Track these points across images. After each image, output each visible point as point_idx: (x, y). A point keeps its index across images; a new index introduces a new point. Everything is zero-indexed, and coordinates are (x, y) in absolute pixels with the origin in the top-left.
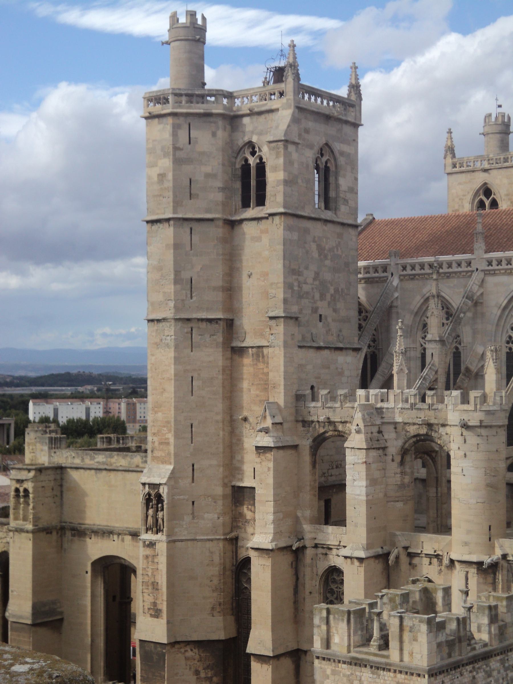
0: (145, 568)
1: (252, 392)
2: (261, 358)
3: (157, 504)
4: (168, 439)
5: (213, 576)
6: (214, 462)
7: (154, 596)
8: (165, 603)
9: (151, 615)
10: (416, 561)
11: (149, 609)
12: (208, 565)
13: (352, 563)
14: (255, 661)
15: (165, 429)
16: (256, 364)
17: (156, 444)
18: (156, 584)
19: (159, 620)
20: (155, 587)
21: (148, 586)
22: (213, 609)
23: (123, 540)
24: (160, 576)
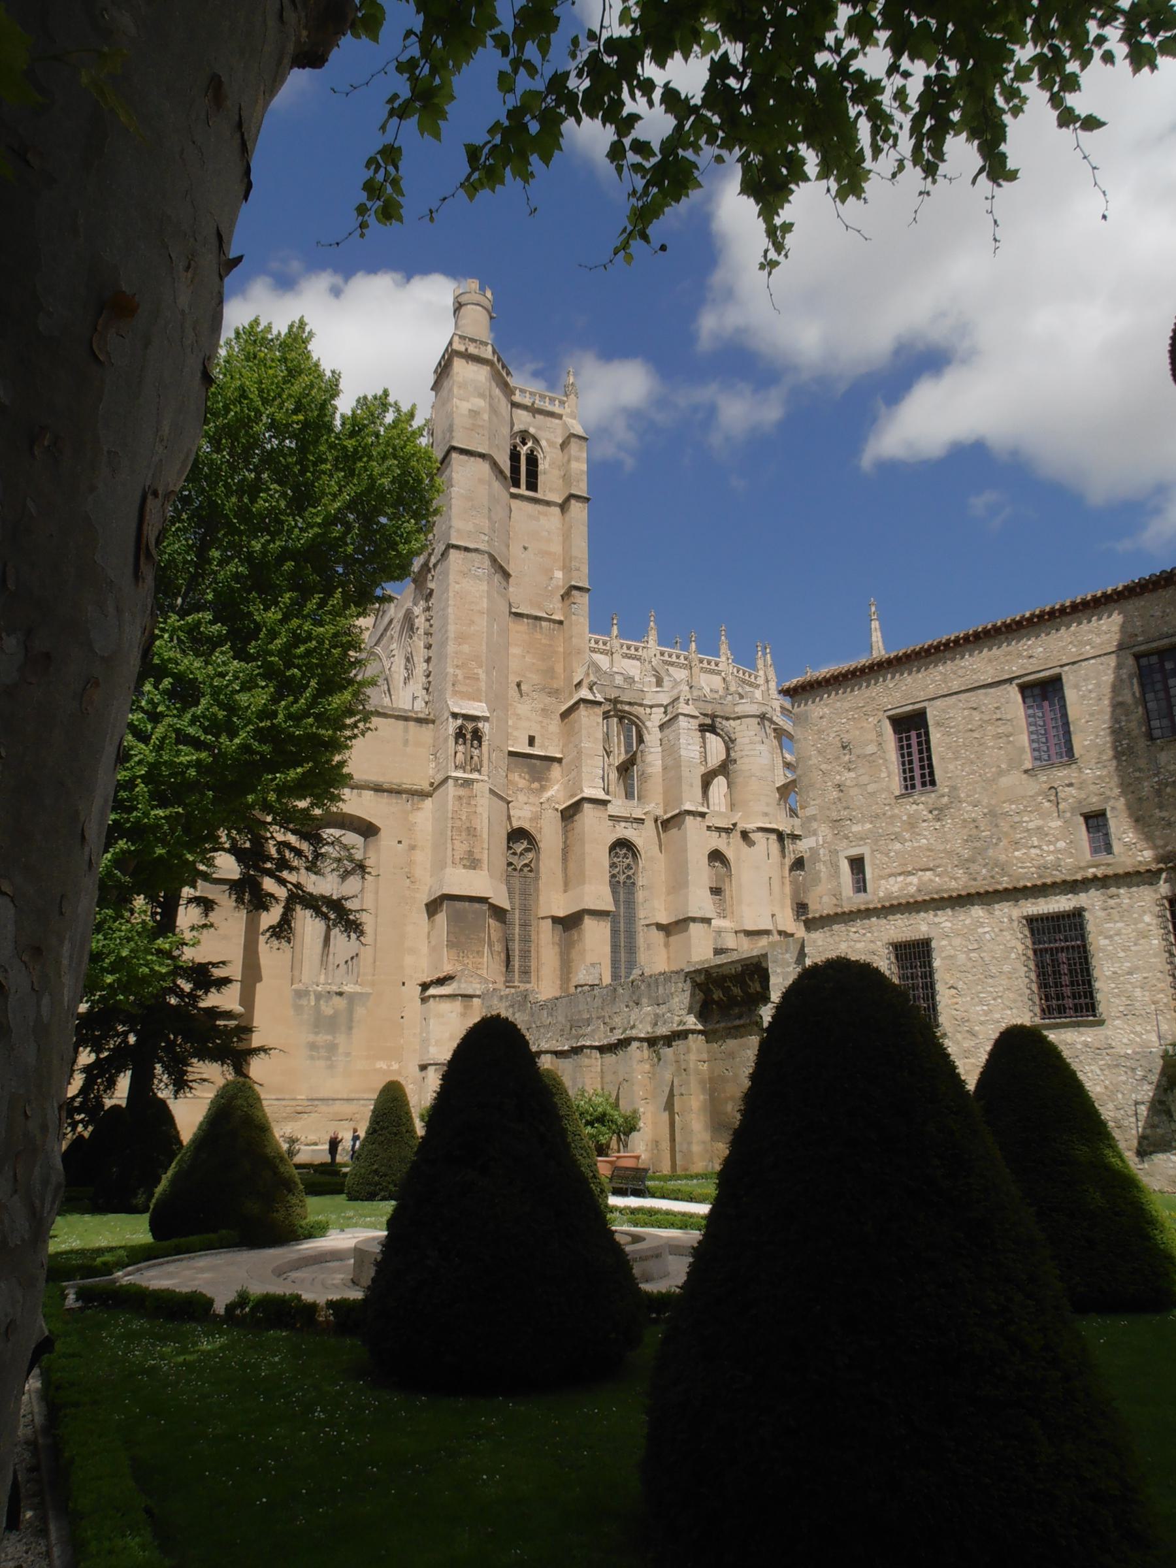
1: (527, 659)
3: (472, 741)
4: (477, 674)
9: (465, 866)
17: (460, 677)
23: (360, 795)
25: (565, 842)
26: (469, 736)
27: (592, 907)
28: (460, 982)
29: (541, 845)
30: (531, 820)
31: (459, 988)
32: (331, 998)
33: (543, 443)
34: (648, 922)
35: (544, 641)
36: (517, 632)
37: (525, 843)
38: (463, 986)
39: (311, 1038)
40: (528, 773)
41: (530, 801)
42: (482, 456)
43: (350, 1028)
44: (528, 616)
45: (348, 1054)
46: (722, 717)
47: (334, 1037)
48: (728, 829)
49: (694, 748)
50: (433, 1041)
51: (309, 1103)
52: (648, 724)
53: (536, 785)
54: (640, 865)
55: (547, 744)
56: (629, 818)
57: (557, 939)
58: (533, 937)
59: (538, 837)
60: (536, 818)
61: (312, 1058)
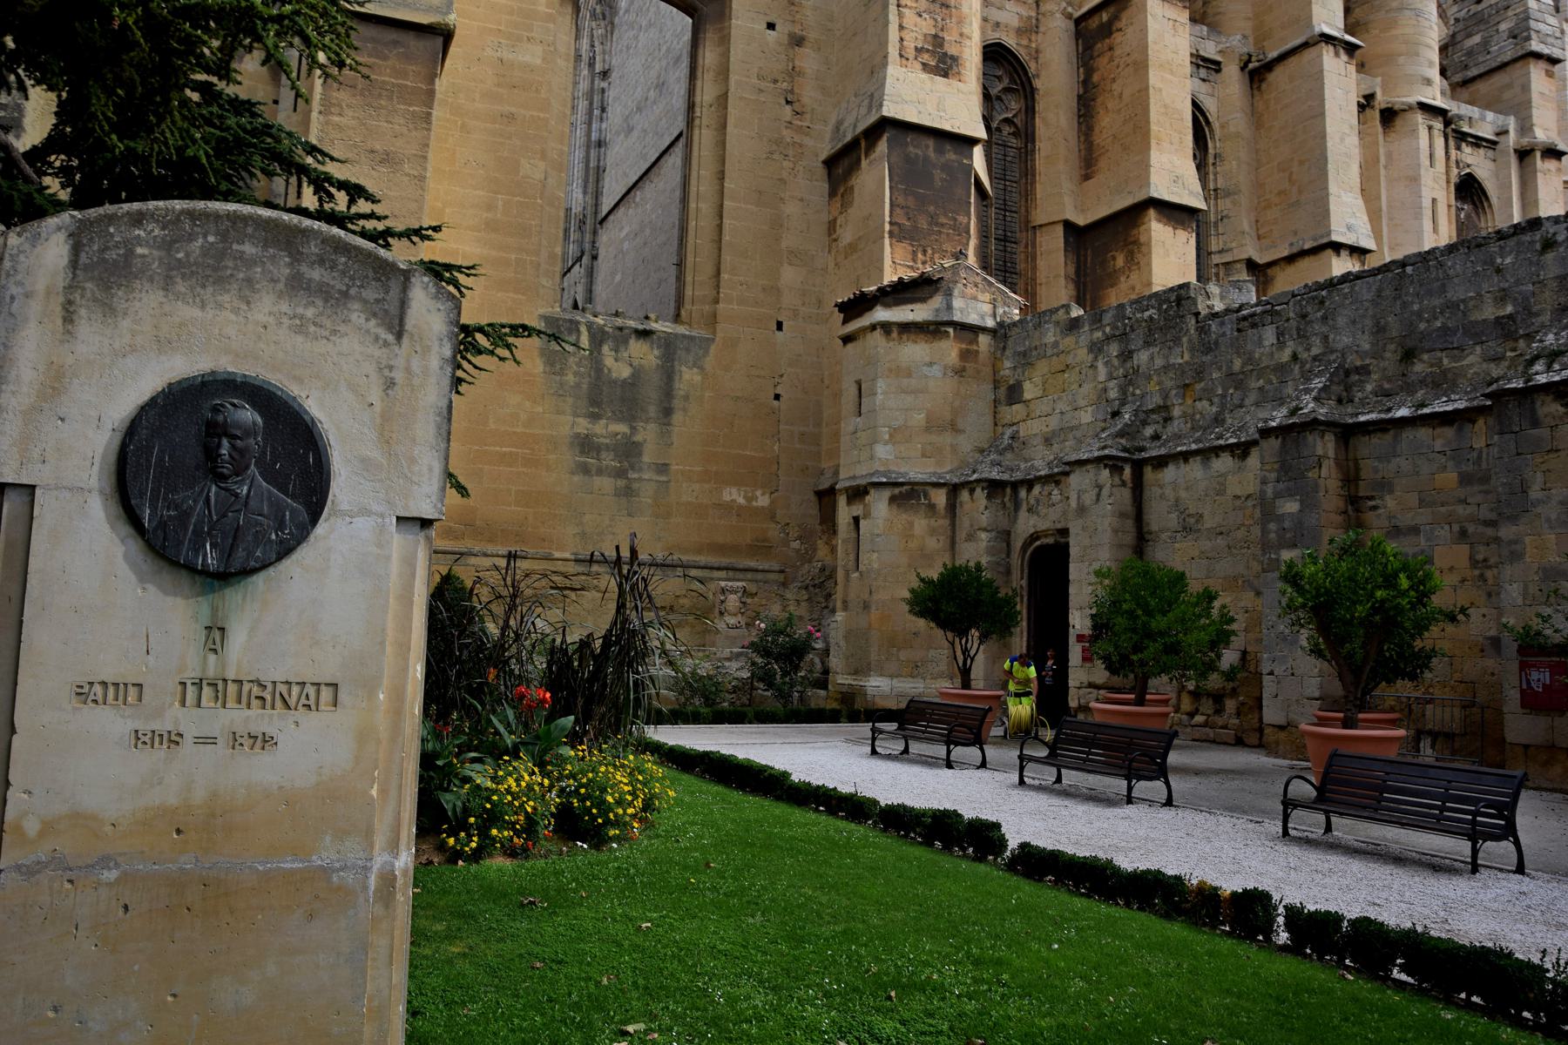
7: (936, 20)
9: (925, 66)
11: (918, 50)
13: (1337, 54)
14: (1159, 221)
19: (953, 82)
25: (1086, 83)
27: (1167, 198)
28: (949, 294)
29: (1037, 83)
30: (1020, 32)
31: (949, 307)
32: (626, 342)
34: (1227, 258)
37: (1006, 81)
38: (957, 303)
39: (583, 425)
43: (667, 412)
45: (663, 468)
47: (633, 428)
50: (884, 433)
51: (580, 569)
54: (1211, 151)
57: (1072, 270)
58: (1021, 266)
59: (1032, 67)
60: (1030, 29)
61: (585, 470)
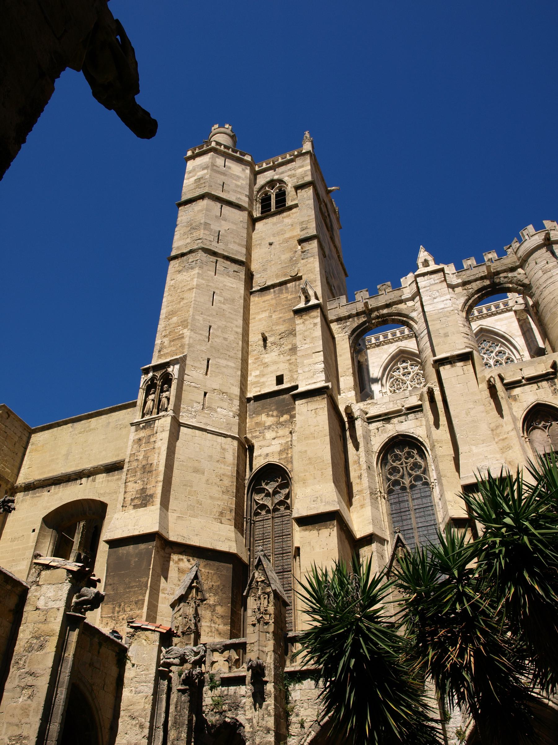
0: (134, 454)
1: (273, 317)
2: (284, 291)
4: (183, 334)
5: (223, 475)
6: (231, 364)
7: (144, 481)
8: (161, 484)
9: (135, 507)
10: (517, 391)
12: (218, 461)
15: (180, 327)
16: (279, 296)
18: (147, 466)
20: (147, 469)
21: (136, 472)
22: (221, 514)
24: (156, 455)
26: (159, 383)
30: (281, 452)
33: (286, 179)
35: (290, 297)
36: (264, 302)
40: (276, 409)
41: (278, 435)
42: (202, 197)
44: (273, 286)
46: (505, 271)
48: (548, 374)
49: (443, 299)
52: (414, 315)
53: (286, 417)
55: (295, 376)
56: (400, 411)
